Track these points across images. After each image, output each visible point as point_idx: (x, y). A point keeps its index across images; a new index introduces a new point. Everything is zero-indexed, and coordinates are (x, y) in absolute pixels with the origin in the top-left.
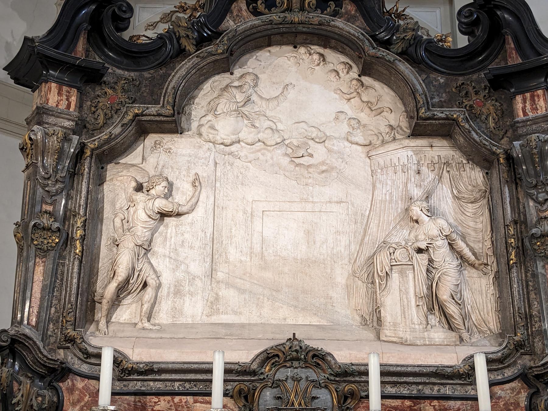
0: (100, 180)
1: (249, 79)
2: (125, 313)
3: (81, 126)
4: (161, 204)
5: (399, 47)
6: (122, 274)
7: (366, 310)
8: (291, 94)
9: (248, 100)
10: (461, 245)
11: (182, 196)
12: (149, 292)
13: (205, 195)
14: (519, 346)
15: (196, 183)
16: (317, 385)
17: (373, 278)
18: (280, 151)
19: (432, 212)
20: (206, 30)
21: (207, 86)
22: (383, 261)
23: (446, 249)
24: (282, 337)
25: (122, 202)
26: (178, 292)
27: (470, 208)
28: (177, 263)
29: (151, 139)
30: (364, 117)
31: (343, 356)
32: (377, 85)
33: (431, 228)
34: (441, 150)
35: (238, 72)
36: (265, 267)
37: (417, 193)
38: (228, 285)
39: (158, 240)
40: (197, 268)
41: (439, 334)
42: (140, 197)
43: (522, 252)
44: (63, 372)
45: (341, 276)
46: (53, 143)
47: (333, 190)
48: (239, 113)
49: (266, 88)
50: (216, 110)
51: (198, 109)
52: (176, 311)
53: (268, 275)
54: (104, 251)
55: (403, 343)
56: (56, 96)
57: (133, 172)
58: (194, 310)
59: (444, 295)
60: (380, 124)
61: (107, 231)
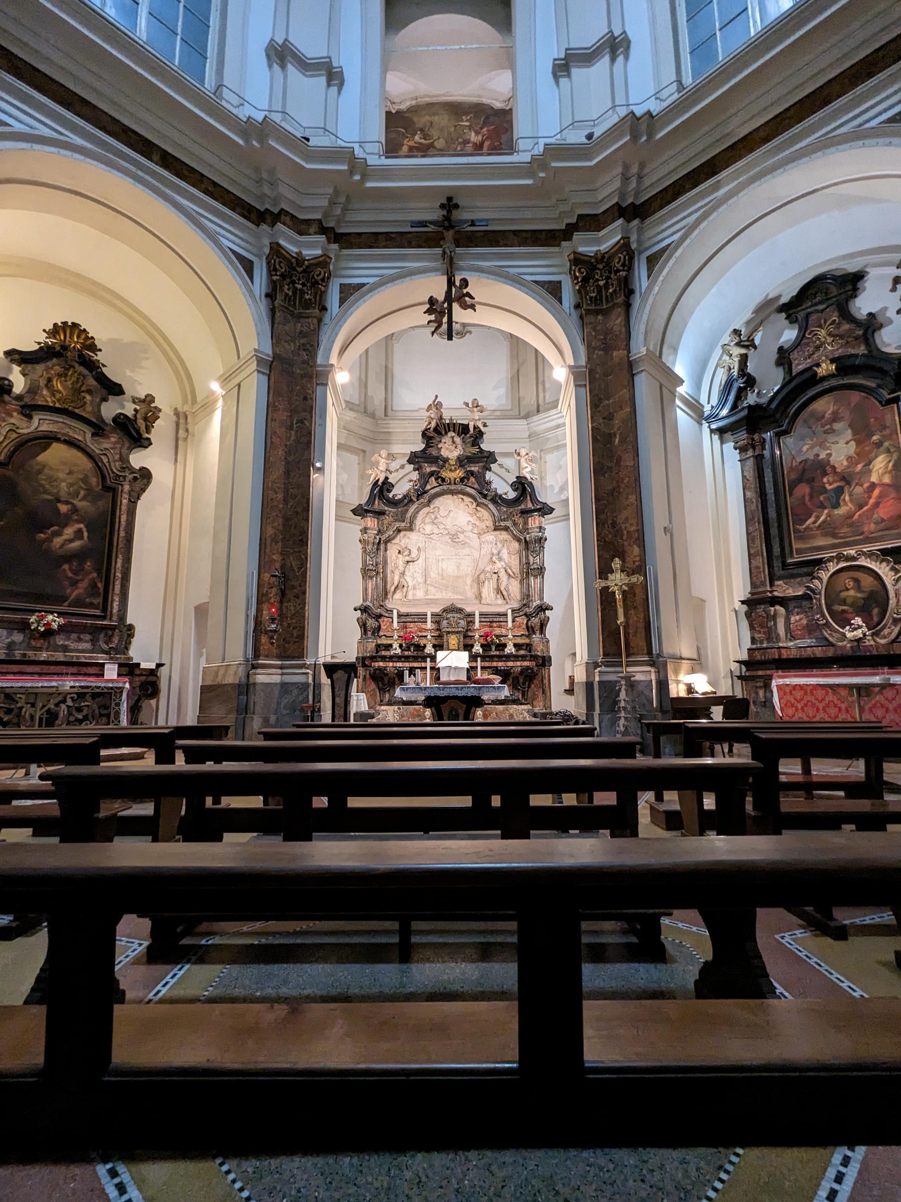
0: (386, 550)
1: (436, 509)
2: (398, 596)
3: (380, 532)
4: (407, 558)
5: (489, 498)
6: (396, 584)
7: (477, 593)
8: (451, 514)
9: (436, 518)
10: (509, 571)
11: (413, 555)
12: (405, 589)
13: (422, 553)
14: (524, 605)
15: (419, 549)
16: (460, 619)
17: (479, 582)
18: (447, 537)
19: (500, 559)
20: (421, 493)
21: (421, 512)
22: (482, 576)
23: (504, 572)
24: (449, 604)
25: (394, 557)
26: (414, 589)
27: (513, 557)
28: (414, 578)
29: (402, 533)
30: (477, 523)
31: (468, 609)
32: (482, 510)
33: (499, 565)
34: (504, 535)
35: (432, 506)
36: (443, 579)
37: (495, 552)
38: (431, 585)
39: (407, 570)
40: (420, 580)
41: (500, 601)
42: (400, 556)
43: (528, 573)
44: (381, 616)
45: (469, 581)
46: (371, 540)
47: (466, 551)
48: (433, 523)
49: (443, 513)
50: (425, 520)
51: (418, 522)
52: (414, 595)
53: (444, 582)
54: (389, 575)
55: (488, 604)
56: (371, 522)
57: (397, 546)
58: (420, 594)
59: (502, 589)
60: (483, 525)
61: (390, 568)
